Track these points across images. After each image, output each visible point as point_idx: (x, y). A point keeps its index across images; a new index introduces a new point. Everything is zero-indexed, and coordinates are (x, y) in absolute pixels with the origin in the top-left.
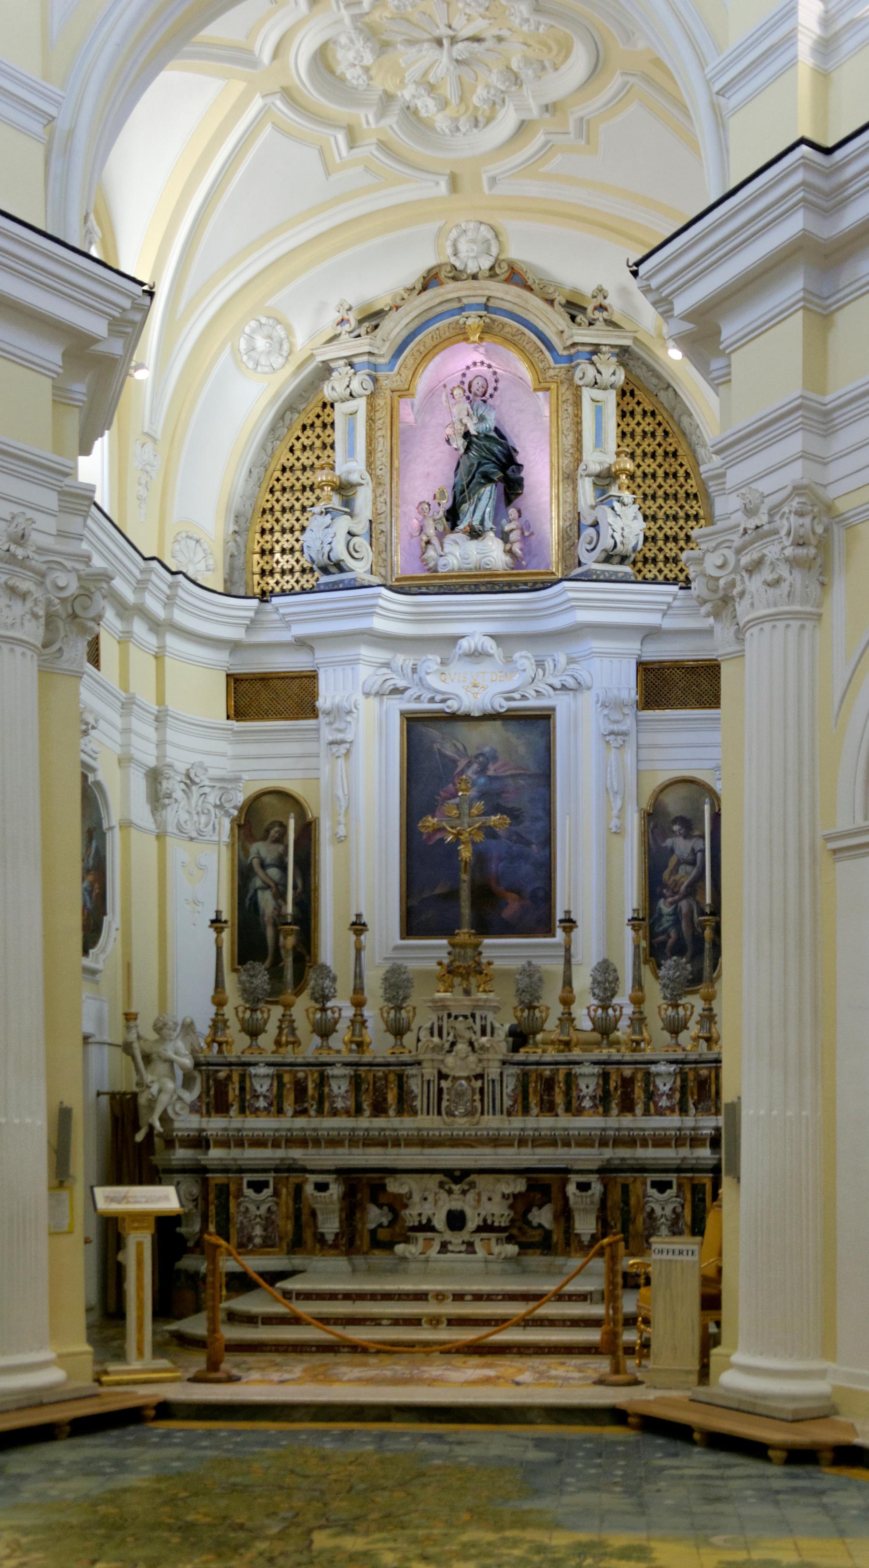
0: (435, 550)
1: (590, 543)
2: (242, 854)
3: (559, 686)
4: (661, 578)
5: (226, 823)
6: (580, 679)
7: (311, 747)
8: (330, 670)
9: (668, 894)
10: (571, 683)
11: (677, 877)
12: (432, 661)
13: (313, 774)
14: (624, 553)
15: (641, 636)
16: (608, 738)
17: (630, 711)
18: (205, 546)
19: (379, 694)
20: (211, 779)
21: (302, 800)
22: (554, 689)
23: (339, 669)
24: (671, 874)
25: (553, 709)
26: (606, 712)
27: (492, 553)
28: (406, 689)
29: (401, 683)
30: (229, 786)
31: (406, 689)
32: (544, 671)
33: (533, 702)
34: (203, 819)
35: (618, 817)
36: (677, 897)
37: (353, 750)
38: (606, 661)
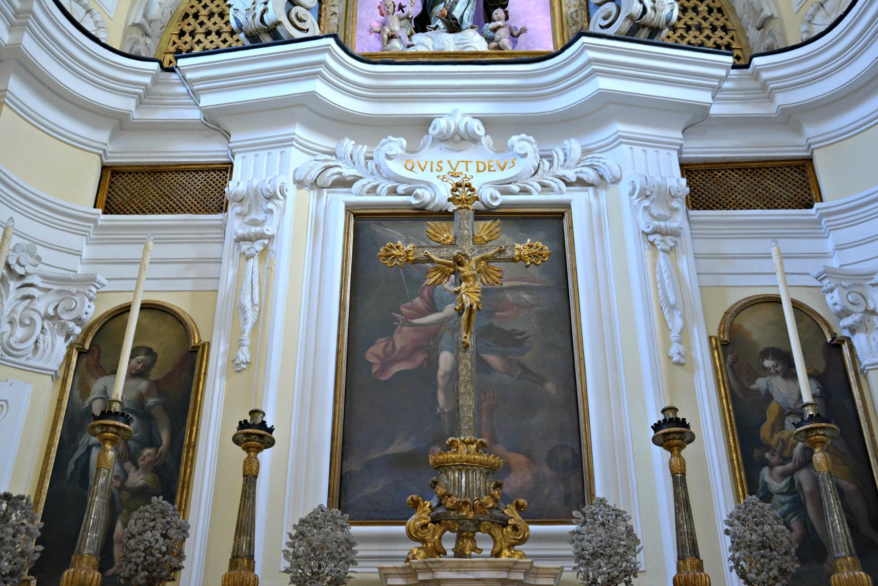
0: (401, 42)
1: (605, 18)
2: (77, 393)
3: (574, 180)
4: (710, 43)
5: (61, 346)
6: (602, 172)
7: (211, 251)
8: (250, 156)
9: (774, 460)
10: (590, 175)
11: (784, 435)
12: (396, 144)
13: (209, 285)
14: (655, 23)
15: (682, 125)
16: (651, 238)
17: (679, 204)
18: (98, 17)
19: (315, 185)
20: (46, 278)
21: (189, 322)
22: (568, 184)
23: (263, 154)
24: (773, 431)
25: (568, 206)
26: (646, 203)
27: (475, 41)
28: (357, 178)
29: (348, 171)
30: (74, 290)
31: (357, 178)
32: (551, 162)
33: (536, 197)
34: (20, 332)
35: (680, 342)
36: (790, 465)
37: (273, 247)
38: (638, 150)
